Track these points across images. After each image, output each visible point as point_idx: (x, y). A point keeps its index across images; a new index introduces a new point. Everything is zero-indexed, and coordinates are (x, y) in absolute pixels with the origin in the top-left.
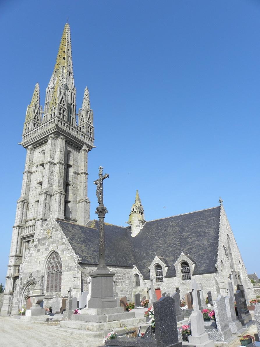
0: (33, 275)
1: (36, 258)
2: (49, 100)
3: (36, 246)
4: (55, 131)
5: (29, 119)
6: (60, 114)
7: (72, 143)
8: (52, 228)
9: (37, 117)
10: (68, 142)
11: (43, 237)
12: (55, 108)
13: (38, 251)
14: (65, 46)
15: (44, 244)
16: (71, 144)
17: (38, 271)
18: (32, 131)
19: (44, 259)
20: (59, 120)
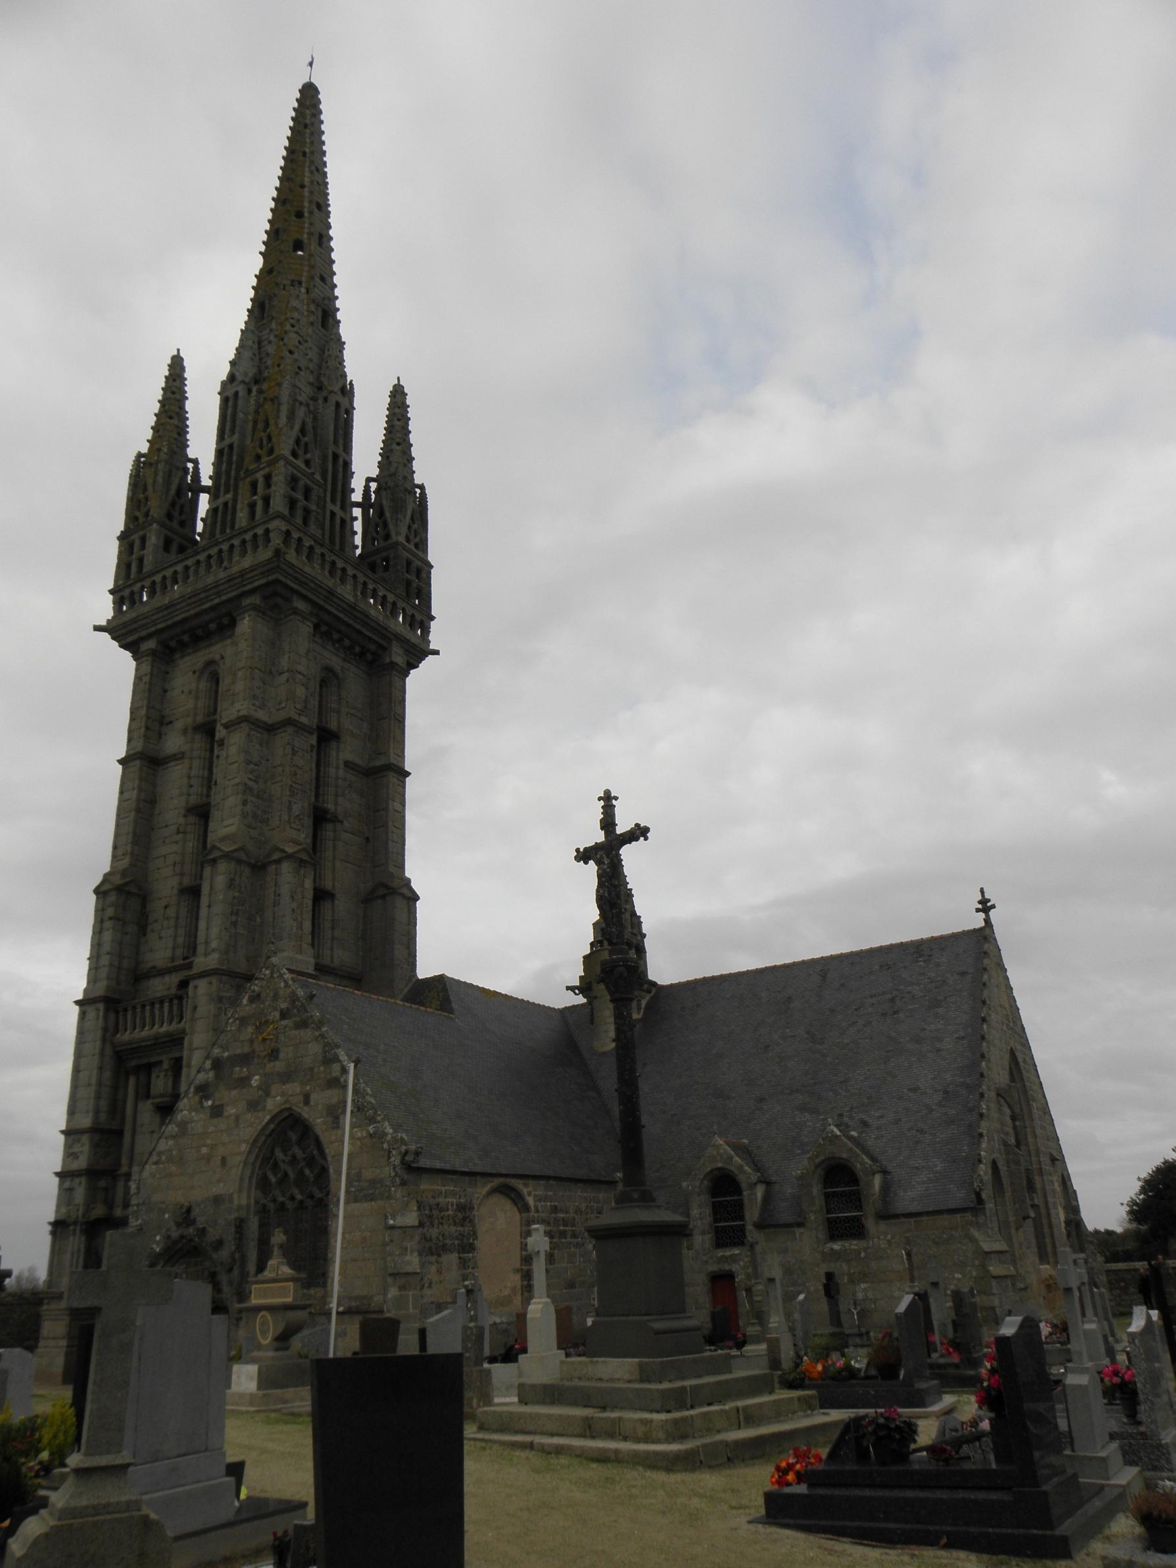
0: (193, 1214)
1: (209, 1141)
2: (236, 436)
3: (203, 1091)
4: (271, 578)
5: (141, 520)
6: (292, 503)
7: (339, 632)
8: (277, 1014)
9: (177, 508)
10: (324, 628)
11: (239, 1051)
12: (268, 478)
13: (217, 1111)
14: (303, 186)
15: (244, 1082)
16: (336, 636)
17: (217, 1200)
18: (158, 572)
19: (244, 1147)
20: (288, 533)
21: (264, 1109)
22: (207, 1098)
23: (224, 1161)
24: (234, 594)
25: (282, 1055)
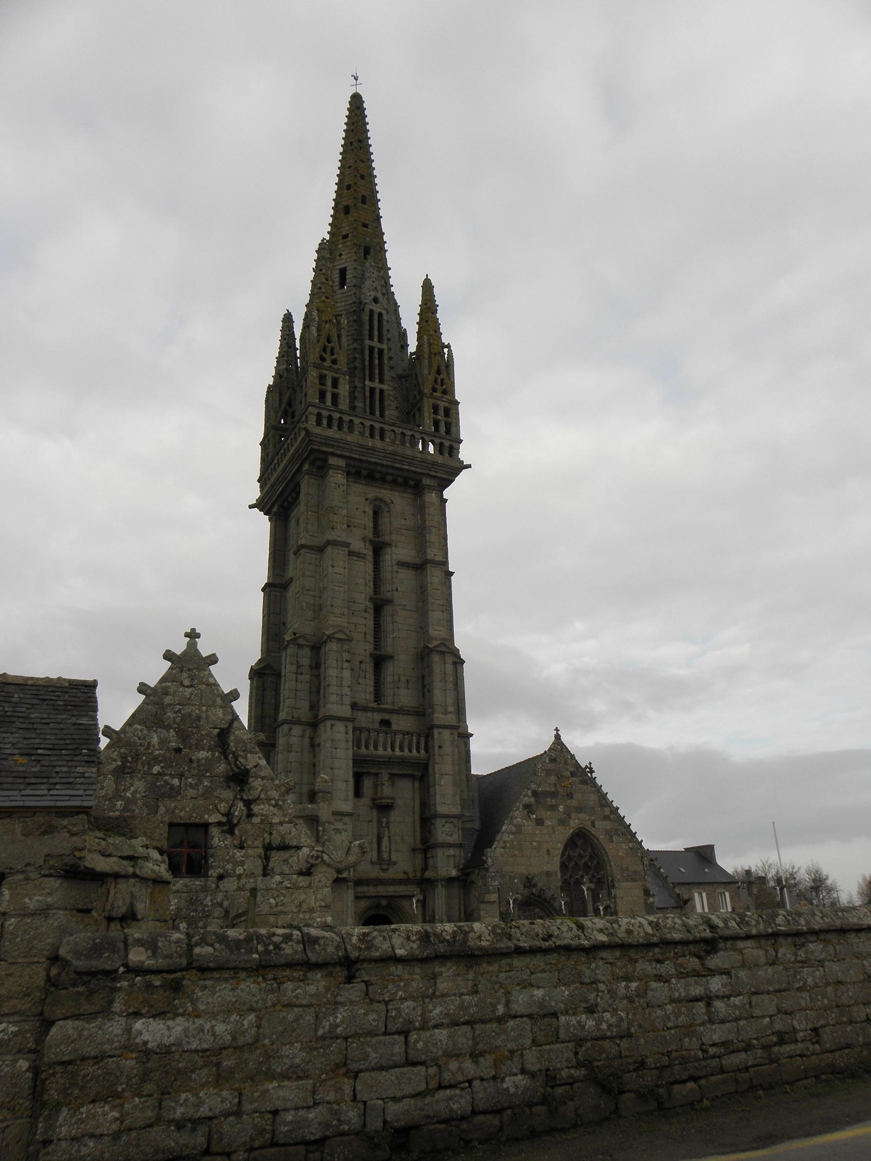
3: (528, 807)
8: (569, 774)
11: (548, 789)
13: (540, 822)
15: (554, 808)
17: (548, 874)
21: (569, 826)
22: (533, 813)
23: (548, 852)
24: (420, 471)
25: (575, 797)
